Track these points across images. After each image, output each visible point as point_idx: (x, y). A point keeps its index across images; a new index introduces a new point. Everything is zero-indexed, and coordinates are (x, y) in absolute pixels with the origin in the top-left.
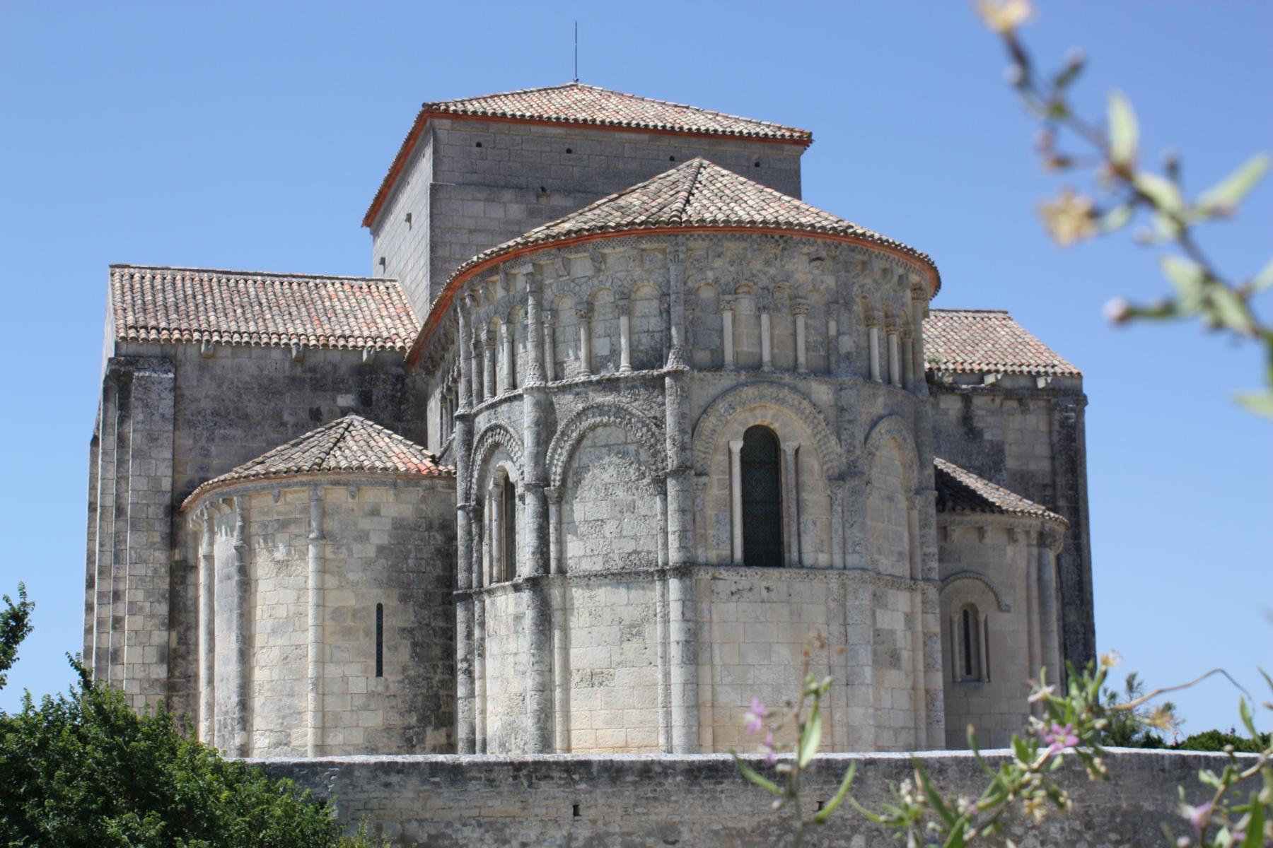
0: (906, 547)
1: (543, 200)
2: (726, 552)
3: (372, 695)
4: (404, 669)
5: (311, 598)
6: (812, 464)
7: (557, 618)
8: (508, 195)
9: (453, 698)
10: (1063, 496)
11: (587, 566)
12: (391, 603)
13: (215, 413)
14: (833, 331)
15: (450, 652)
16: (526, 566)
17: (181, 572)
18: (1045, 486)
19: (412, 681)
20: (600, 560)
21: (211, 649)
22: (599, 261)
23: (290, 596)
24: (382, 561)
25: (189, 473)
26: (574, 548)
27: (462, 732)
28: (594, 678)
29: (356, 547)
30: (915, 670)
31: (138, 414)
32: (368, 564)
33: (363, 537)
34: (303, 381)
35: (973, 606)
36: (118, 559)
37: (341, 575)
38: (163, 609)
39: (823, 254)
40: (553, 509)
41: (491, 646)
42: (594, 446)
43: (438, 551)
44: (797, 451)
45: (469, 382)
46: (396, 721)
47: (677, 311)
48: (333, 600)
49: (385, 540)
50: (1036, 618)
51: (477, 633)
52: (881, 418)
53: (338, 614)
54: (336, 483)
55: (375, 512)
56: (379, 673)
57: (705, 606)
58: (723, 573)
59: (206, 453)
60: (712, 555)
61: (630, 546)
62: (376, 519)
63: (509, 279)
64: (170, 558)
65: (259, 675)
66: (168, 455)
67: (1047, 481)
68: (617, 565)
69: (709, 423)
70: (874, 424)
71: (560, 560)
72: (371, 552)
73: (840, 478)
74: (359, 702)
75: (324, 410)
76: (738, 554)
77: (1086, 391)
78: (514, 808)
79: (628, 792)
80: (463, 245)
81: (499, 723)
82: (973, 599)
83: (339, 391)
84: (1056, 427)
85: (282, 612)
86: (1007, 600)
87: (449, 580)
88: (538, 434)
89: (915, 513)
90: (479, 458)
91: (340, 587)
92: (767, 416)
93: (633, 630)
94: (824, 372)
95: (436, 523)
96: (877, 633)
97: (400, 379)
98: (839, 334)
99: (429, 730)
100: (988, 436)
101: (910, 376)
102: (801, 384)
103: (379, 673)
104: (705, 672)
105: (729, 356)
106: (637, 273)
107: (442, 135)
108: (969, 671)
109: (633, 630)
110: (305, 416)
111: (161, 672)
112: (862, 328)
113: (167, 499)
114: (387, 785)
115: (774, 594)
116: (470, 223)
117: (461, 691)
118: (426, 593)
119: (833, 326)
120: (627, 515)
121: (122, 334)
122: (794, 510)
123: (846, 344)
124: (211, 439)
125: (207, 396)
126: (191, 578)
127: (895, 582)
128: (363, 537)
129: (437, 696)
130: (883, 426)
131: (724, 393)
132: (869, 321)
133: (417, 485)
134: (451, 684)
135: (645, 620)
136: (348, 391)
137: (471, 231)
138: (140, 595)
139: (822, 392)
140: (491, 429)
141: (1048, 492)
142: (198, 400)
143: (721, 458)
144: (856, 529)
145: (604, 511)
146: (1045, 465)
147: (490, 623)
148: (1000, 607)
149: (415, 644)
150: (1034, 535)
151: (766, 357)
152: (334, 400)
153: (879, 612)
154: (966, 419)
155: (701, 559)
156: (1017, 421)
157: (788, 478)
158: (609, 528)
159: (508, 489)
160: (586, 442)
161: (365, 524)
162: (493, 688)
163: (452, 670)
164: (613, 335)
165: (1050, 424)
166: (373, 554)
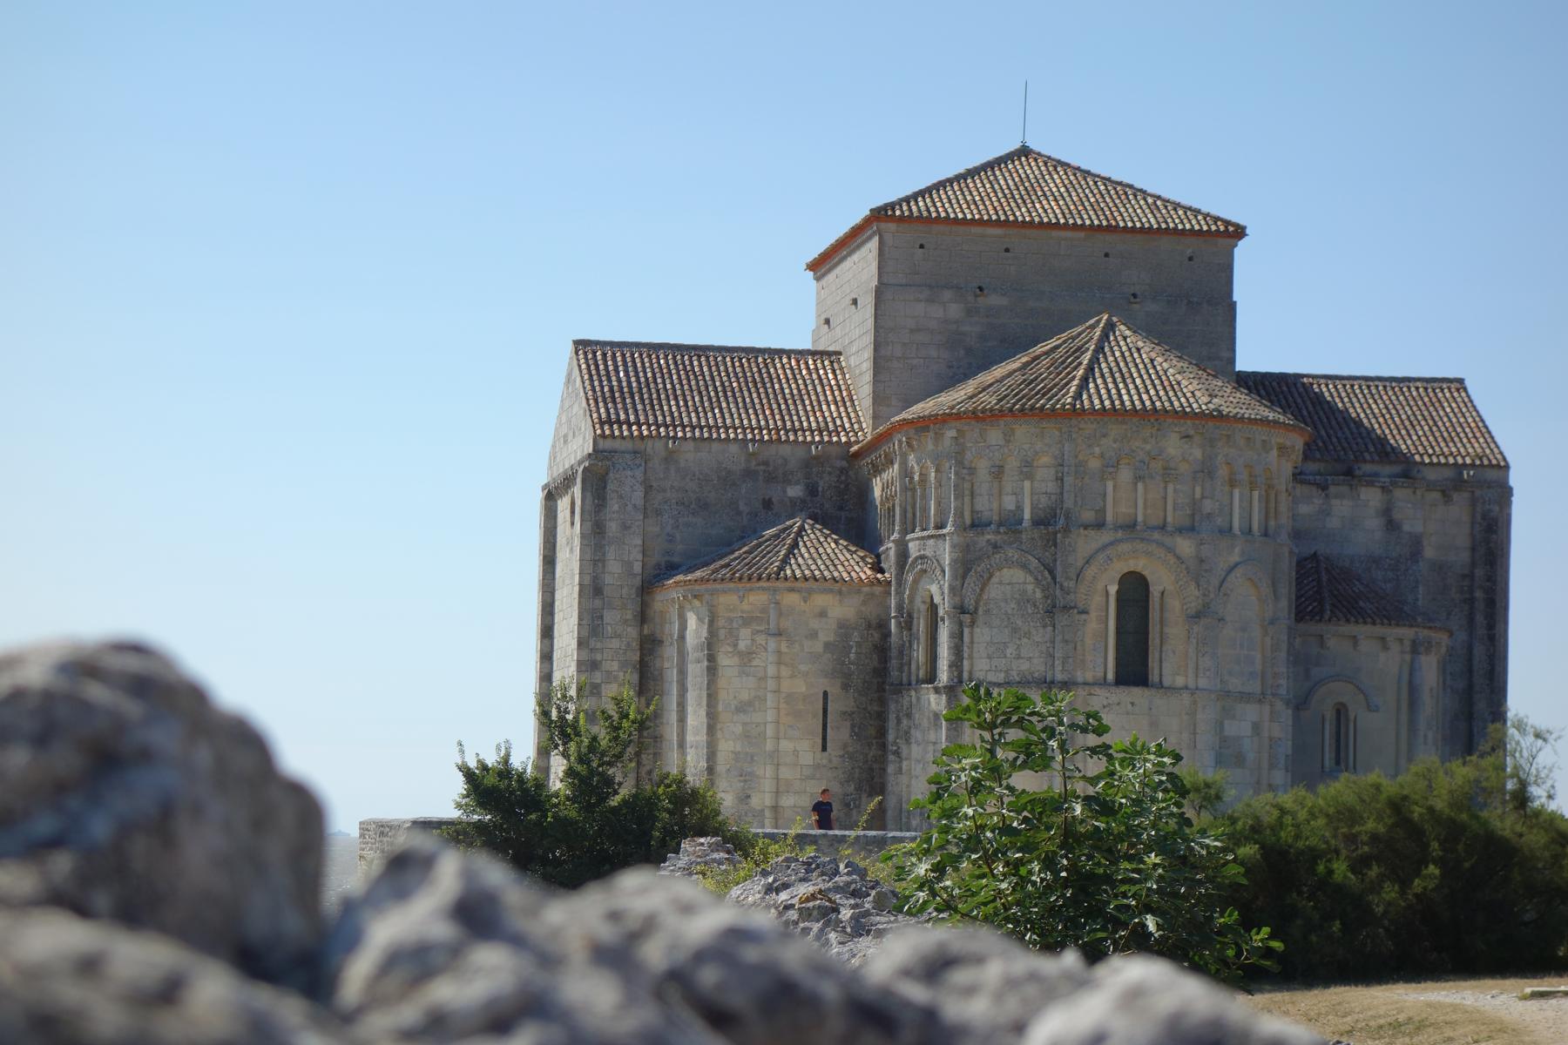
0: (1258, 667)
3: (817, 767)
4: (845, 746)
6: (1174, 605)
8: (947, 295)
9: (884, 770)
12: (834, 690)
13: (680, 503)
14: (1198, 496)
15: (882, 733)
16: (944, 676)
17: (649, 646)
20: (1002, 675)
21: (682, 720)
22: (1008, 436)
27: (891, 802)
31: (614, 505)
33: (813, 635)
35: (1343, 705)
38: (635, 678)
39: (1192, 432)
40: (966, 631)
41: (916, 734)
42: (1001, 583)
47: (1068, 480)
48: (786, 686)
50: (1404, 717)
51: (905, 722)
52: (1236, 565)
54: (792, 590)
55: (823, 614)
56: (824, 748)
58: (1097, 690)
60: (1089, 676)
61: (1025, 666)
63: (938, 437)
66: (640, 542)
69: (1090, 572)
70: (1231, 570)
73: (1198, 616)
76: (1111, 676)
77: (1512, 482)
80: (904, 344)
85: (745, 696)
87: (881, 672)
89: (1268, 640)
91: (791, 677)
92: (1139, 565)
94: (1189, 529)
95: (874, 623)
96: (1224, 740)
97: (842, 470)
100: (1406, 528)
101: (1272, 523)
102: (1168, 540)
103: (824, 748)
105: (1109, 518)
106: (1039, 446)
107: (888, 238)
108: (1338, 763)
112: (1227, 488)
113: (638, 581)
117: (891, 769)
119: (1198, 490)
122: (1158, 641)
123: (1208, 506)
125: (672, 487)
127: (1245, 697)
128: (813, 635)
129: (872, 769)
130: (1238, 572)
131: (1105, 547)
132: (1232, 483)
133: (859, 591)
134: (882, 761)
136: (797, 483)
137: (912, 331)
138: (615, 666)
139: (1185, 546)
140: (922, 557)
142: (664, 491)
143: (1098, 599)
146: (1465, 556)
148: (1371, 708)
149: (853, 726)
150: (1407, 643)
151: (1140, 519)
152: (785, 492)
154: (1387, 511)
155: (1080, 680)
157: (1154, 615)
159: (933, 608)
160: (994, 580)
161: (815, 624)
165: (1473, 516)
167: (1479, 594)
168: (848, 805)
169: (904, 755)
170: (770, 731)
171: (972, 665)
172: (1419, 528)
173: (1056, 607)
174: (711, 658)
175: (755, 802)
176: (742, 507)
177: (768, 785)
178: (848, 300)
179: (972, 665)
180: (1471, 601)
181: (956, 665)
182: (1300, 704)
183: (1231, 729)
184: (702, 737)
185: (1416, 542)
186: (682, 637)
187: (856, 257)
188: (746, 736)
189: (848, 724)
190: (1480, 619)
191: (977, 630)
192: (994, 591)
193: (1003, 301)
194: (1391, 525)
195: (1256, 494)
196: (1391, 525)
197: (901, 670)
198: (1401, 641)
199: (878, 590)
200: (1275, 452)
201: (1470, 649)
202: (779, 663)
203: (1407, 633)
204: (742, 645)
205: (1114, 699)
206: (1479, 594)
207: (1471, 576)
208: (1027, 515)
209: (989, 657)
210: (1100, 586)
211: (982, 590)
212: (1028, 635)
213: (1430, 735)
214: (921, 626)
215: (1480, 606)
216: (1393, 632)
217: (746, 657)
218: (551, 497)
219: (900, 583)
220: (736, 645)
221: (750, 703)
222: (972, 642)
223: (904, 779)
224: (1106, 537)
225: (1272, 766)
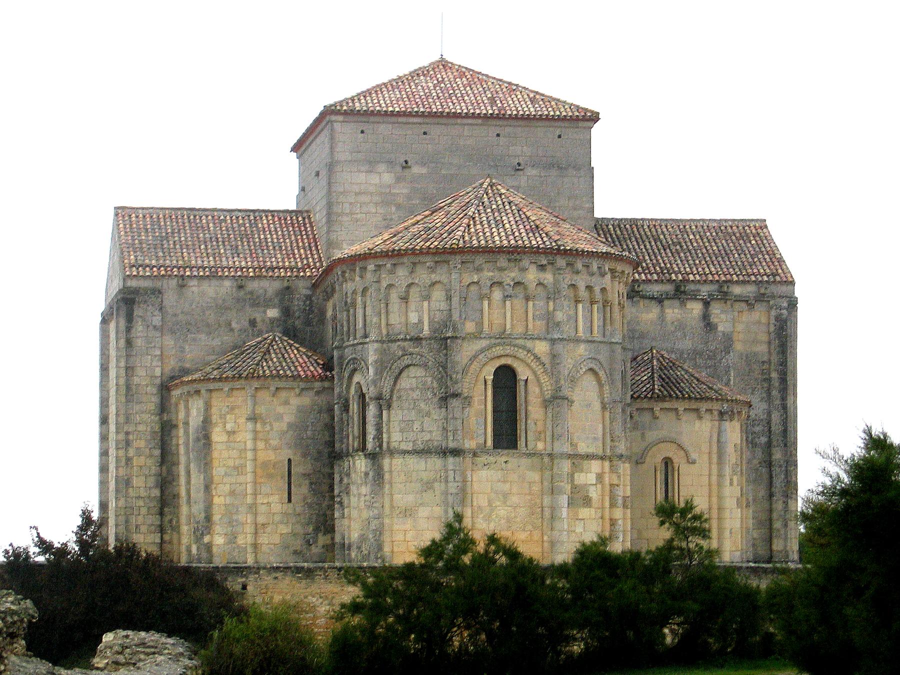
1: (407, 171)
2: (482, 441)
3: (285, 514)
4: (305, 498)
5: (250, 455)
6: (534, 389)
7: (387, 476)
11: (404, 446)
12: (296, 459)
15: (331, 488)
16: (370, 446)
17: (166, 429)
18: (763, 362)
19: (310, 506)
21: (188, 482)
23: (234, 453)
25: (172, 364)
26: (396, 437)
27: (338, 539)
28: (408, 513)
29: (276, 425)
30: (603, 508)
31: (139, 328)
32: (284, 433)
33: (279, 417)
34: (245, 300)
35: (670, 459)
36: (128, 421)
37: (266, 441)
38: (157, 452)
39: (544, 262)
40: (384, 412)
41: (353, 488)
43: (326, 425)
45: (342, 326)
46: (299, 529)
48: (262, 456)
50: (715, 467)
51: (345, 480)
53: (265, 465)
56: (290, 500)
59: (182, 350)
61: (427, 437)
64: (161, 419)
65: (216, 500)
67: (765, 359)
72: (284, 427)
74: (277, 518)
75: (258, 320)
76: (490, 443)
77: (796, 295)
80: (351, 204)
81: (356, 535)
82: (670, 455)
83: (267, 306)
84: (773, 321)
85: (231, 463)
86: (694, 456)
87: (331, 444)
88: (377, 369)
89: (607, 414)
90: (346, 375)
91: (266, 449)
93: (428, 486)
96: (574, 487)
97: (309, 298)
98: (554, 310)
99: (320, 535)
100: (720, 328)
102: (529, 344)
103: (290, 500)
107: (337, 126)
109: (428, 486)
110: (247, 324)
111: (156, 492)
112: (573, 304)
113: (158, 381)
114: (276, 578)
115: (509, 465)
116: (356, 188)
117: (337, 515)
118: (319, 452)
120: (426, 418)
121: (128, 273)
122: (523, 415)
123: (560, 316)
124: (185, 341)
126: (174, 432)
127: (589, 457)
128: (279, 417)
129: (325, 515)
131: (482, 351)
132: (577, 302)
134: (331, 508)
135: (435, 480)
136: (274, 307)
137: (357, 194)
138: (142, 444)
139: (541, 348)
141: (766, 366)
144: (559, 428)
145: (413, 415)
147: (353, 475)
149: (311, 484)
151: (508, 326)
152: (265, 312)
153: (576, 475)
154: (706, 317)
156: (746, 317)
158: (416, 426)
159: (362, 396)
161: (281, 409)
162: (355, 514)
163: (333, 498)
164: (419, 310)
166: (285, 428)
167: (774, 375)
168: (308, 541)
169: (346, 504)
171: (389, 438)
174: (207, 437)
175: (241, 541)
176: (234, 325)
177: (249, 529)
178: (314, 174)
179: (389, 438)
180: (769, 380)
181: (379, 437)
182: (638, 461)
183: (581, 478)
184: (201, 495)
186: (186, 423)
187: (318, 141)
188: (232, 493)
189: (307, 482)
190: (775, 393)
192: (405, 383)
193: (424, 171)
194: (708, 324)
195: (595, 307)
197: (341, 442)
198: (709, 411)
199: (327, 384)
200: (609, 276)
201: (769, 414)
202: (255, 439)
203: (716, 406)
205: (492, 459)
206: (774, 375)
207: (770, 362)
208: (426, 328)
209: (402, 431)
210: (481, 378)
212: (428, 414)
213: (735, 478)
214: (354, 407)
216: (704, 406)
218: (105, 321)
219: (341, 379)
221: (236, 468)
222: (389, 421)
223: (346, 522)
224: (484, 343)
225: (613, 505)
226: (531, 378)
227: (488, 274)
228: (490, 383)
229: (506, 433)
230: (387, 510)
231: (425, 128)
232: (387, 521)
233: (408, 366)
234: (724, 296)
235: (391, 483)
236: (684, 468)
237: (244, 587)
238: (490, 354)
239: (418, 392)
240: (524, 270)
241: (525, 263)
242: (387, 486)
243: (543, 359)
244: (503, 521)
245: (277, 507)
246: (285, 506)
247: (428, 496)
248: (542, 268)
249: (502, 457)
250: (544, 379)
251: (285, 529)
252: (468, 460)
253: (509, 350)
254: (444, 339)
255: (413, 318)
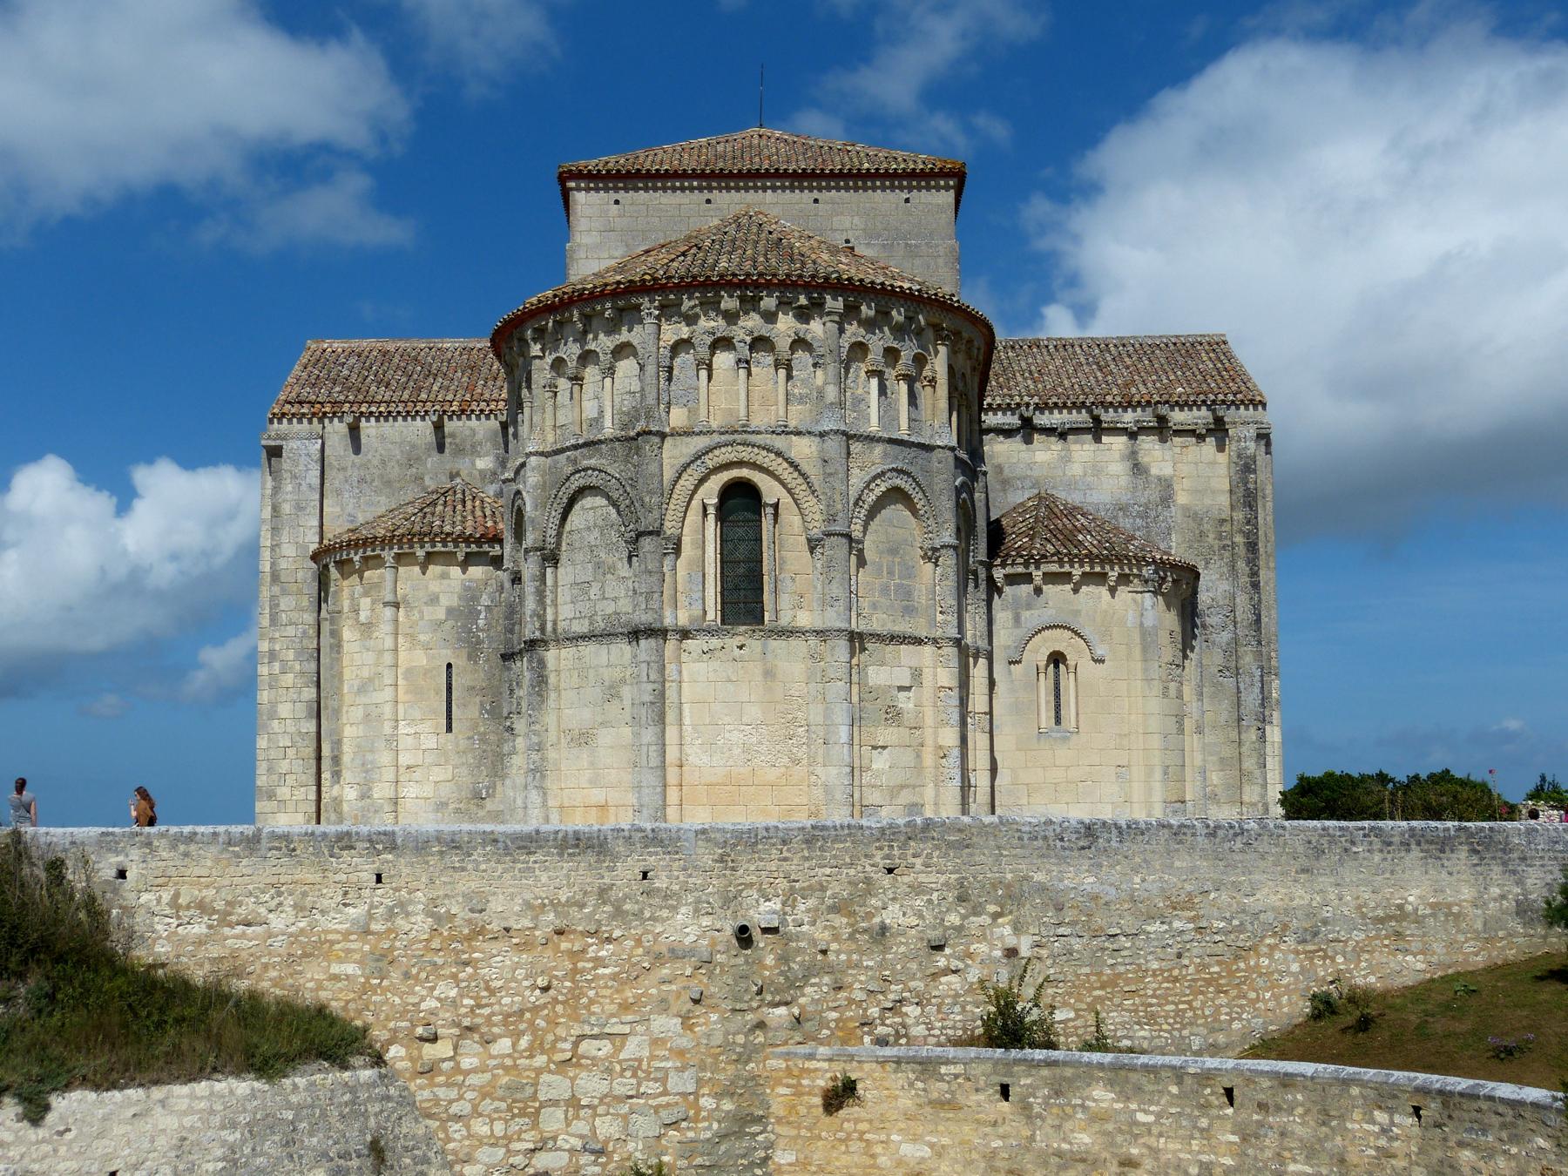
5: (388, 658)
6: (790, 518)
7: (552, 679)
10: (1241, 531)
12: (460, 663)
20: (587, 622)
24: (451, 623)
26: (566, 611)
28: (583, 739)
33: (434, 600)
44: (776, 506)
49: (455, 602)
53: (409, 672)
56: (449, 729)
57: (671, 669)
60: (683, 619)
61: (610, 608)
62: (445, 582)
68: (600, 625)
71: (555, 623)
74: (430, 758)
76: (713, 615)
78: (317, 877)
79: (432, 860)
85: (365, 673)
100: (1154, 471)
102: (779, 442)
103: (449, 729)
104: (671, 733)
114: (186, 855)
120: (609, 576)
128: (434, 600)
135: (623, 681)
138: (291, 655)
146: (1224, 500)
152: (473, 464)
158: (594, 590)
167: (1239, 539)
170: (387, 710)
172: (1167, 470)
173: (644, 536)
177: (389, 775)
185: (1166, 485)
191: (561, 570)
192: (576, 519)
194: (1138, 469)
196: (1138, 469)
204: (363, 617)
205: (715, 642)
211: (564, 518)
212: (612, 569)
215: (1241, 551)
217: (367, 628)
220: (357, 620)
221: (371, 680)
226: (786, 499)
227: (709, 324)
228: (711, 510)
229: (744, 598)
230: (552, 736)
231: (706, 195)
232: (552, 754)
233: (581, 492)
234: (1162, 429)
235: (557, 689)
236: (1086, 667)
237: (122, 874)
238: (710, 461)
239: (596, 533)
240: (770, 317)
241: (769, 302)
242: (553, 695)
243: (805, 467)
244: (737, 751)
245: (430, 742)
246: (446, 738)
247: (613, 708)
248: (803, 315)
249: (745, 644)
250: (810, 503)
251: (439, 774)
252: (671, 645)
253: (745, 454)
254: (638, 437)
255: (590, 409)
